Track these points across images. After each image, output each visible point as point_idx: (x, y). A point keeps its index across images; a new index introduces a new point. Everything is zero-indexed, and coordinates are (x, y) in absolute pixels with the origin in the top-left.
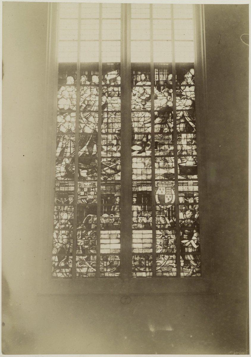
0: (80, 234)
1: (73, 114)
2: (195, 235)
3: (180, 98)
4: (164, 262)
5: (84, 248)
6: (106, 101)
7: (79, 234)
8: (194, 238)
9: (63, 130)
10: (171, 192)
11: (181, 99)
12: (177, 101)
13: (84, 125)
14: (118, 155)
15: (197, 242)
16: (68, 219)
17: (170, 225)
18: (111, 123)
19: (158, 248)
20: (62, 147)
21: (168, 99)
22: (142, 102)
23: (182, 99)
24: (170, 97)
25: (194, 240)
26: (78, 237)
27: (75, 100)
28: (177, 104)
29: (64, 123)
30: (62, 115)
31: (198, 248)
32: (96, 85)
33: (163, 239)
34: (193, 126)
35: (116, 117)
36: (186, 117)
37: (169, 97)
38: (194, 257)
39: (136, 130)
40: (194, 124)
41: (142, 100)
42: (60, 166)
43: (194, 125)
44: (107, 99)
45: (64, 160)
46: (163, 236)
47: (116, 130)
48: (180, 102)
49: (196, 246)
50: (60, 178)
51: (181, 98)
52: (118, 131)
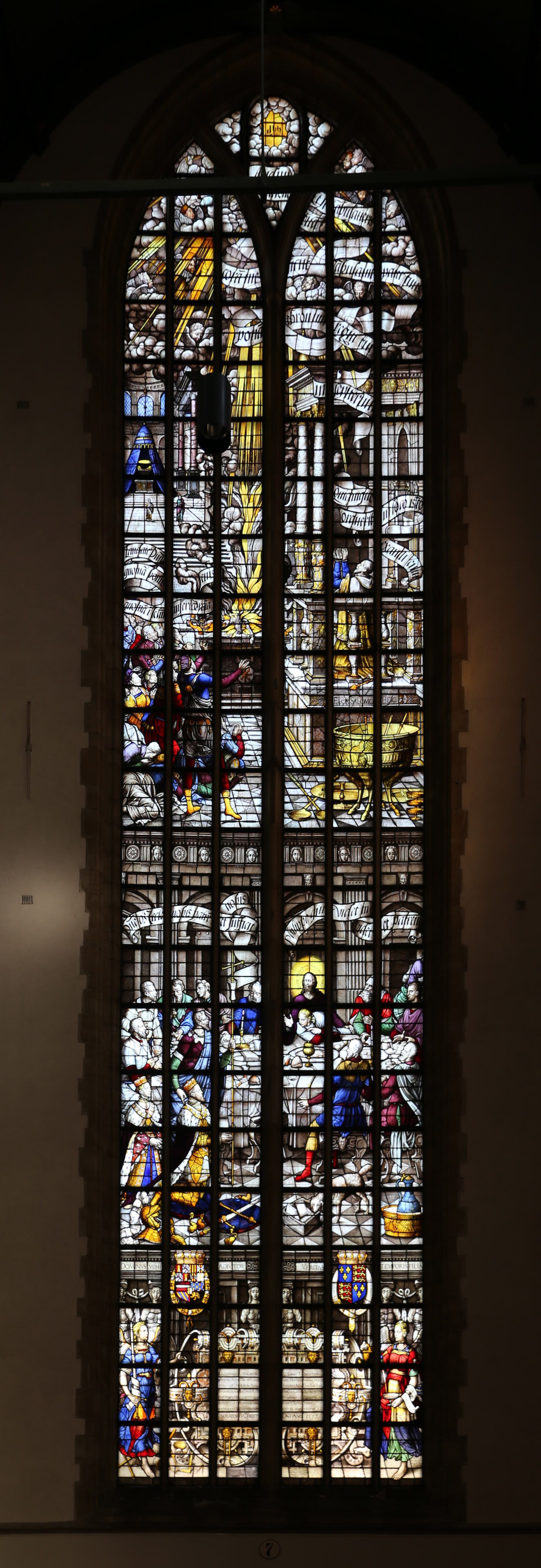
0: (176, 1376)
1: (157, 1081)
2: (413, 1381)
3: (390, 1040)
4: (346, 1443)
5: (184, 1408)
6: (230, 1045)
7: (173, 1375)
8: (411, 1388)
9: (135, 1119)
10: (365, 1278)
11: (393, 1043)
12: (384, 1046)
13: (181, 1105)
14: (254, 1183)
15: (417, 1399)
16: (149, 1341)
17: (360, 1355)
18: (240, 1102)
19: (335, 1409)
20: (132, 1163)
21: (363, 1040)
22: (305, 1047)
23: (396, 1042)
24: (367, 1035)
25: (410, 1394)
26: (171, 1382)
27: (159, 1042)
28: (384, 1056)
29: (137, 1102)
30: (133, 1083)
31: (417, 1411)
32: (204, 1005)
33: (346, 1389)
34: (416, 1113)
35: (251, 1087)
36: (402, 1087)
37: (365, 1035)
38: (409, 1433)
39: (292, 1121)
40: (419, 1108)
41: (304, 1042)
42: (128, 1211)
43: (418, 1110)
44: (232, 1041)
45: (137, 1196)
46: (346, 1383)
47: (251, 1121)
48: (390, 1051)
49: (413, 1409)
50: (131, 1239)
51: (392, 1039)
52: (256, 1122)
